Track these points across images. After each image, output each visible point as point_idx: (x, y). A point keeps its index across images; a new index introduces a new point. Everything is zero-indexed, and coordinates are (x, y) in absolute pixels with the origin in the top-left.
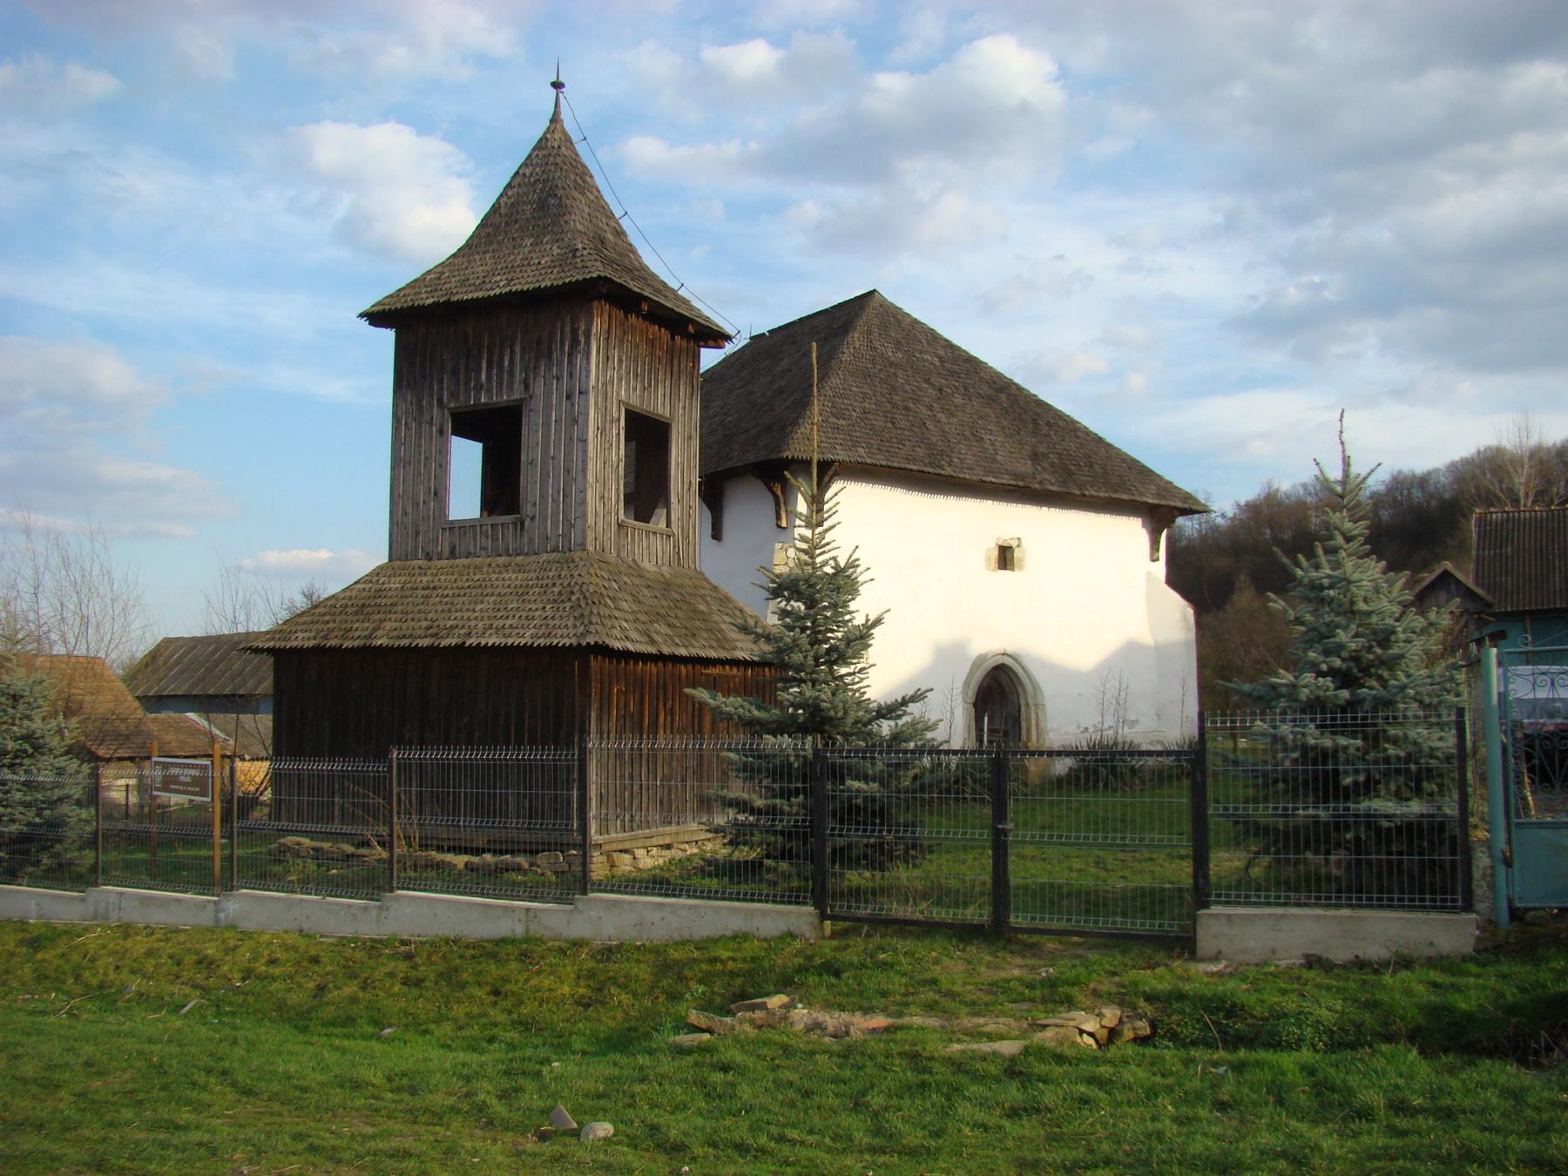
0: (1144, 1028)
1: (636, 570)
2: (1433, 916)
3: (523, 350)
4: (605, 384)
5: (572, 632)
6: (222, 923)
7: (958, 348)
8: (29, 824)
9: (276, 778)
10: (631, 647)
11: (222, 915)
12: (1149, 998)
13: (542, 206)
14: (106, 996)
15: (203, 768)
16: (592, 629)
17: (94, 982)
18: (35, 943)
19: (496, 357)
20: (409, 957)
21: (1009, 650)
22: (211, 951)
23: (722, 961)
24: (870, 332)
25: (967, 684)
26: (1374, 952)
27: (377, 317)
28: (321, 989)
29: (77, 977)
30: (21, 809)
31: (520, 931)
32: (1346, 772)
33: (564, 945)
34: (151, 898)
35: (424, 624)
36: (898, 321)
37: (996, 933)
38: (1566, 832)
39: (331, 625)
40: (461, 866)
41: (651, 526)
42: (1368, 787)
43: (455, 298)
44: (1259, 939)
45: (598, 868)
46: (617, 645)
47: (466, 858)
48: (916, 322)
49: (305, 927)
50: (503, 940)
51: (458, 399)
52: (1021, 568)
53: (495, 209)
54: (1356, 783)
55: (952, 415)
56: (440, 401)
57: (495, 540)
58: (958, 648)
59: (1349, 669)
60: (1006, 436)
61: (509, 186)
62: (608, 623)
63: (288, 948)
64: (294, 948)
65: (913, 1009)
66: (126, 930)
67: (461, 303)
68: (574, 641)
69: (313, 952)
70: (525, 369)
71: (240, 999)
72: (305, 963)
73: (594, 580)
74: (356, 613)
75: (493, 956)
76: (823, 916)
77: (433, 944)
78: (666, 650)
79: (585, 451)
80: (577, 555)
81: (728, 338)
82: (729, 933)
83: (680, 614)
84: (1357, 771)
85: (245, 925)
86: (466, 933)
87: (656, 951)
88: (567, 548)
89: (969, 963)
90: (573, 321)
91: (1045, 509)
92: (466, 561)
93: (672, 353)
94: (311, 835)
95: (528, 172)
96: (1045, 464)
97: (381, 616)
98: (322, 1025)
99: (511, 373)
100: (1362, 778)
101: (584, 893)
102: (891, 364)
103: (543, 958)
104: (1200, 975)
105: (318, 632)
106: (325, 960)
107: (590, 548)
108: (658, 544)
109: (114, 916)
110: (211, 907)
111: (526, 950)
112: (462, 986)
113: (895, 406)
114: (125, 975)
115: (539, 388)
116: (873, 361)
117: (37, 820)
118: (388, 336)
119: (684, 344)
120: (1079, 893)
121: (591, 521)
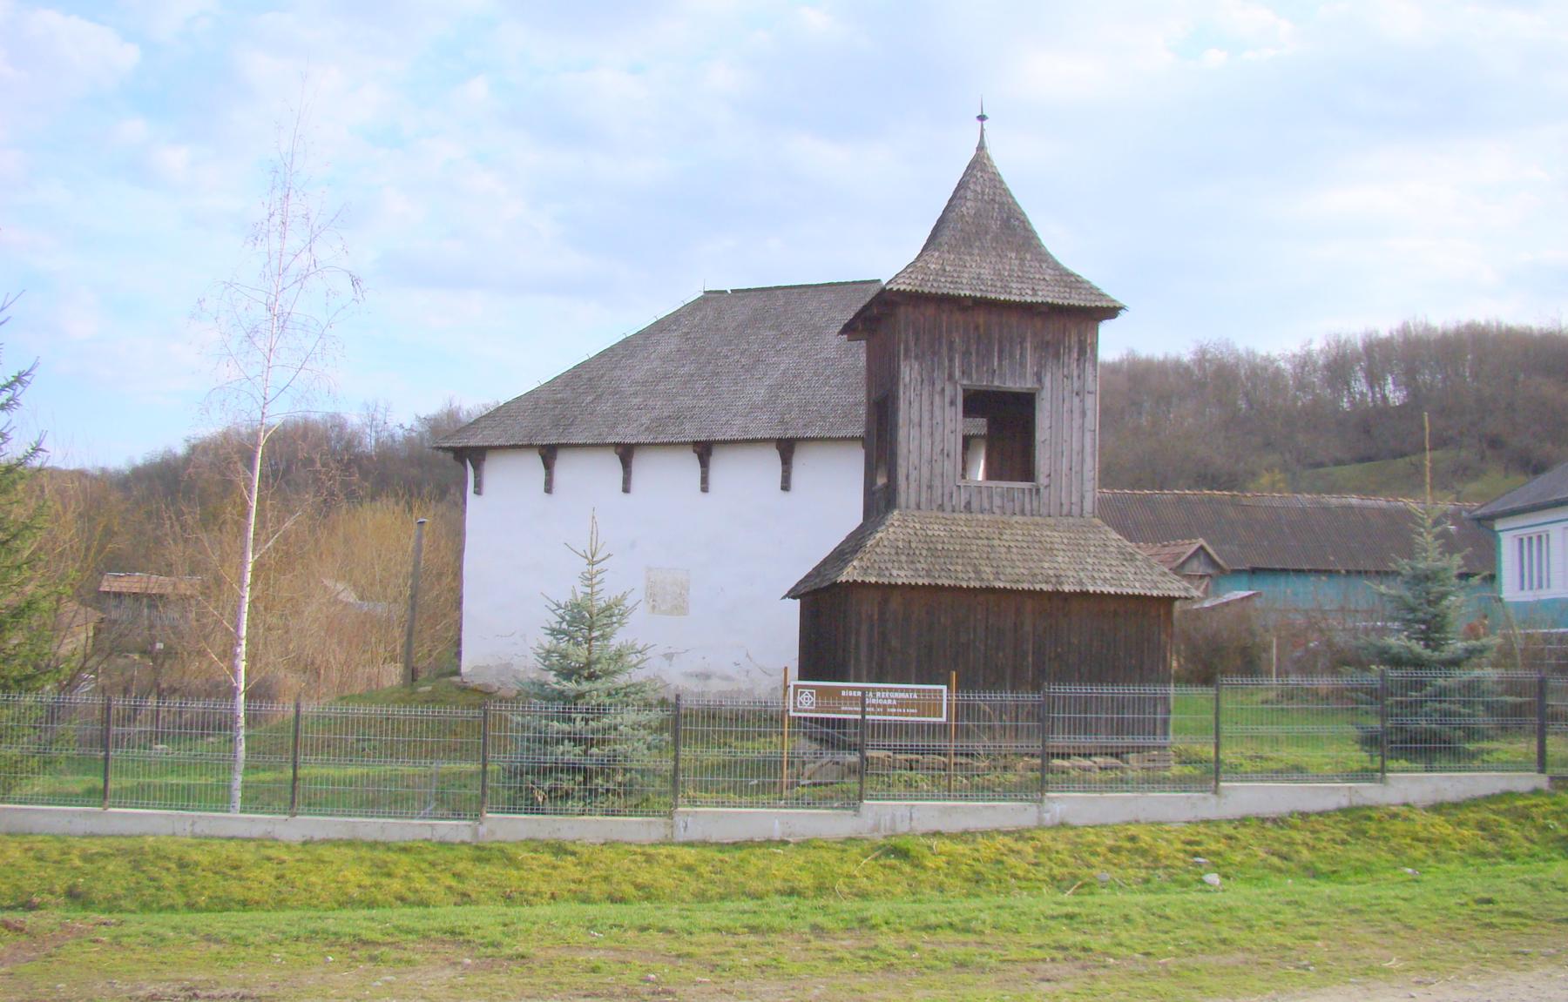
11: (1047, 816)
31: (1345, 803)
51: (970, 377)
56: (951, 377)
85: (1072, 821)
99: (1022, 365)
115: (1047, 381)
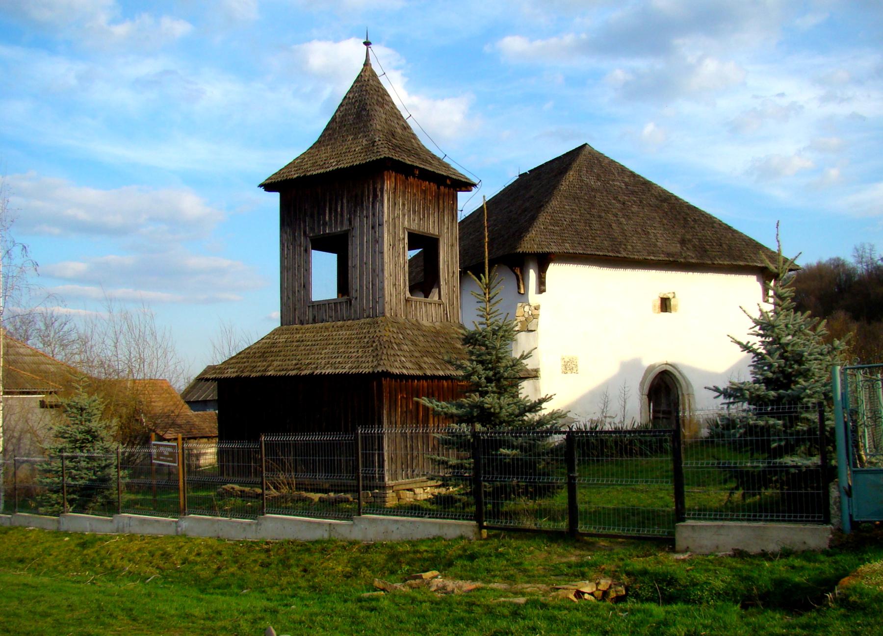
0: (622, 591)
1: (418, 326)
2: (808, 526)
3: (348, 202)
4: (394, 219)
5: (370, 365)
6: (180, 533)
7: (638, 176)
8: (90, 480)
9: (220, 453)
10: (405, 372)
11: (179, 529)
12: (628, 574)
13: (359, 116)
14: (112, 573)
15: (173, 447)
16: (381, 363)
17: (109, 566)
18: (84, 545)
19: (333, 206)
20: (268, 551)
21: (669, 361)
22: (169, 549)
23: (420, 553)
24: (580, 171)
25: (642, 384)
26: (771, 547)
27: (269, 186)
28: (219, 568)
29: (102, 563)
30: (85, 471)
31: (326, 536)
32: (774, 441)
33: (345, 544)
34: (144, 520)
35: (294, 362)
36: (600, 162)
37: (571, 537)
38: (882, 476)
39: (246, 364)
40: (317, 500)
41: (429, 300)
42: (789, 449)
43: (309, 174)
44: (711, 540)
45: (391, 500)
46: (396, 371)
47: (320, 495)
48: (613, 162)
49: (220, 534)
50: (317, 542)
52: (676, 311)
53: (333, 119)
54: (779, 446)
55: (630, 219)
57: (336, 311)
58: (636, 363)
59: (778, 378)
60: (665, 229)
61: (341, 105)
62: (393, 359)
63: (207, 546)
64: (211, 547)
65: (496, 579)
66: (131, 538)
67: (311, 176)
68: (371, 370)
69: (220, 549)
70: (349, 213)
71: (178, 575)
72: (214, 555)
73: (388, 334)
74: (260, 357)
75: (308, 550)
76: (481, 527)
77: (282, 544)
78: (429, 373)
79: (383, 259)
80: (379, 319)
81: (467, 186)
82: (431, 537)
83: (442, 350)
84: (780, 440)
85: (191, 534)
86: (300, 537)
87: (392, 548)
88: (375, 314)
89: (549, 553)
90: (374, 183)
91: (690, 274)
92: (321, 325)
93: (438, 196)
94: (241, 484)
95: (351, 96)
96: (689, 246)
97: (272, 358)
98: (214, 588)
99: (342, 215)
100: (783, 443)
101: (359, 515)
102: (593, 190)
103: (333, 551)
104: (669, 562)
105: (239, 368)
106: (224, 553)
107: (388, 315)
108: (433, 310)
109: (127, 530)
110: (174, 524)
111: (323, 547)
112: (289, 567)
113: (592, 215)
114: (125, 562)
115: (357, 223)
116: (581, 189)
117: (94, 477)
118: (275, 197)
119: (447, 190)
120: (643, 512)
121: (387, 299)
